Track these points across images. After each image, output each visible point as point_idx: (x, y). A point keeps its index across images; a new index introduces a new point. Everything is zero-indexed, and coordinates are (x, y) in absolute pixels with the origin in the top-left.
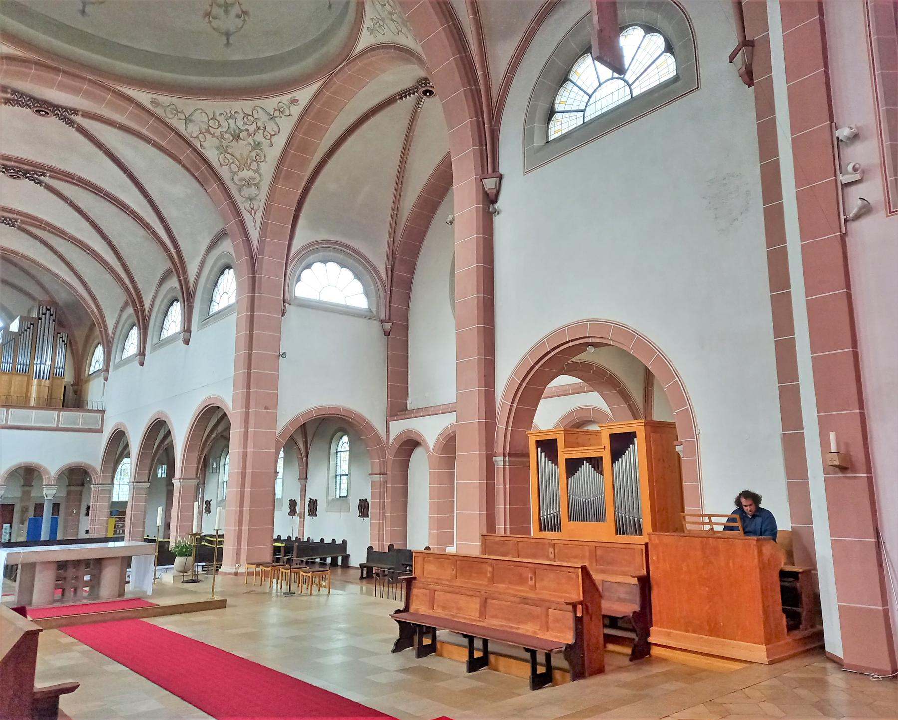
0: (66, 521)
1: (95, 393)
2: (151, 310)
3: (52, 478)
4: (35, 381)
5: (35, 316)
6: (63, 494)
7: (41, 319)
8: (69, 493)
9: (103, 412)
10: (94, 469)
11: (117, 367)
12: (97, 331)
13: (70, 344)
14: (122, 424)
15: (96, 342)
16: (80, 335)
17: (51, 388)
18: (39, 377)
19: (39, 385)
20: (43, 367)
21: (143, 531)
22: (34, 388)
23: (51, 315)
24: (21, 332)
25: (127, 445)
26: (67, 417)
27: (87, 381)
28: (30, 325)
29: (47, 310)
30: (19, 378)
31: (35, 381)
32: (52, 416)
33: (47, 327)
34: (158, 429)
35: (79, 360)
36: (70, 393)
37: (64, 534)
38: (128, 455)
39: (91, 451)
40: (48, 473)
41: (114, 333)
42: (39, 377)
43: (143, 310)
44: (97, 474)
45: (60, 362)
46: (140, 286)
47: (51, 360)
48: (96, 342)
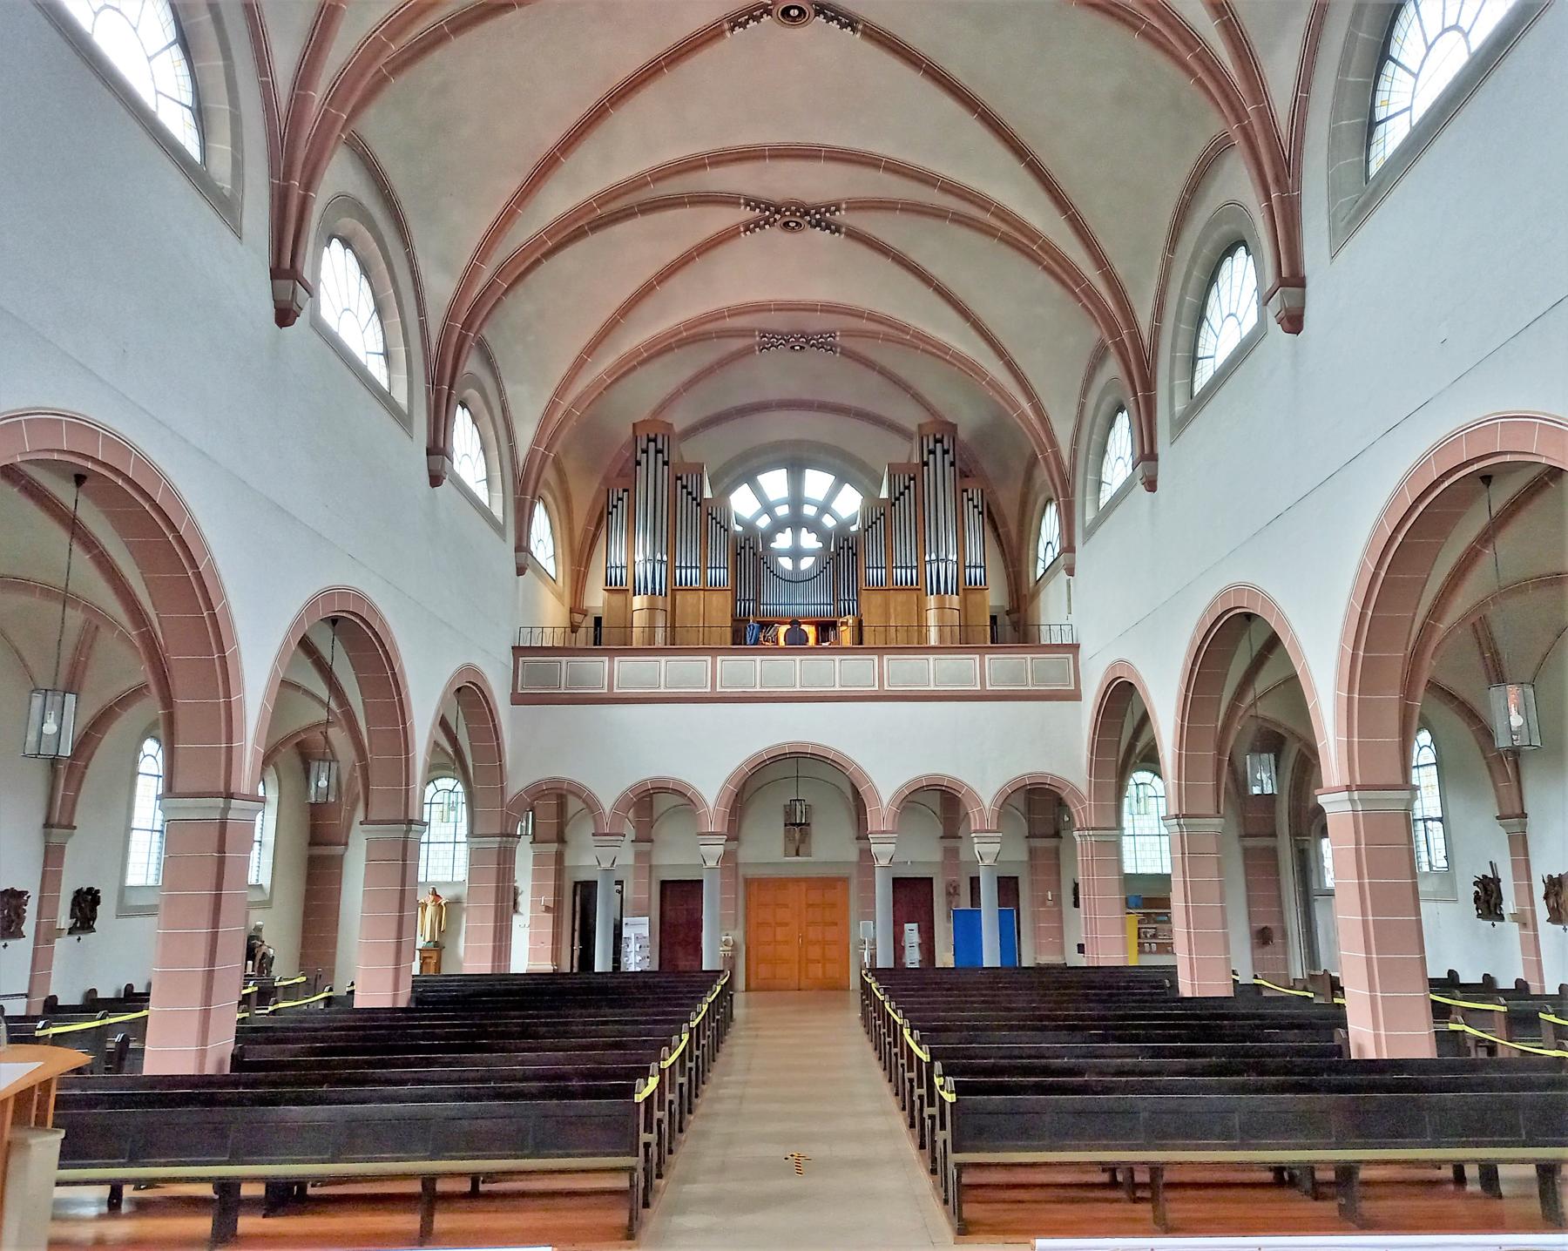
0: (1035, 917)
1: (1054, 613)
2: (1156, 332)
3: (988, 814)
4: (932, 601)
5: (916, 460)
6: (1024, 857)
7: (926, 464)
8: (1032, 852)
9: (1074, 648)
10: (1075, 791)
11: (1089, 532)
12: (1041, 475)
13: (991, 518)
14: (1121, 663)
15: (1041, 500)
16: (1007, 500)
17: (964, 610)
18: (938, 592)
19: (941, 608)
20: (942, 566)
21: (1228, 960)
22: (932, 618)
23: (945, 452)
24: (895, 499)
25: (1145, 718)
26: (998, 667)
27: (1035, 594)
28: (908, 481)
29: (936, 441)
30: (901, 597)
31: (932, 601)
32: (965, 669)
33: (940, 475)
34: (1240, 645)
35: (1013, 549)
36: (1004, 621)
37: (1038, 949)
38: (1150, 760)
39: (1063, 745)
40: (979, 802)
41: (1074, 453)
42: (938, 592)
43: (1136, 336)
44: (1081, 802)
45: (974, 554)
46: (1120, 270)
47: (959, 552)
48: (1041, 500)
